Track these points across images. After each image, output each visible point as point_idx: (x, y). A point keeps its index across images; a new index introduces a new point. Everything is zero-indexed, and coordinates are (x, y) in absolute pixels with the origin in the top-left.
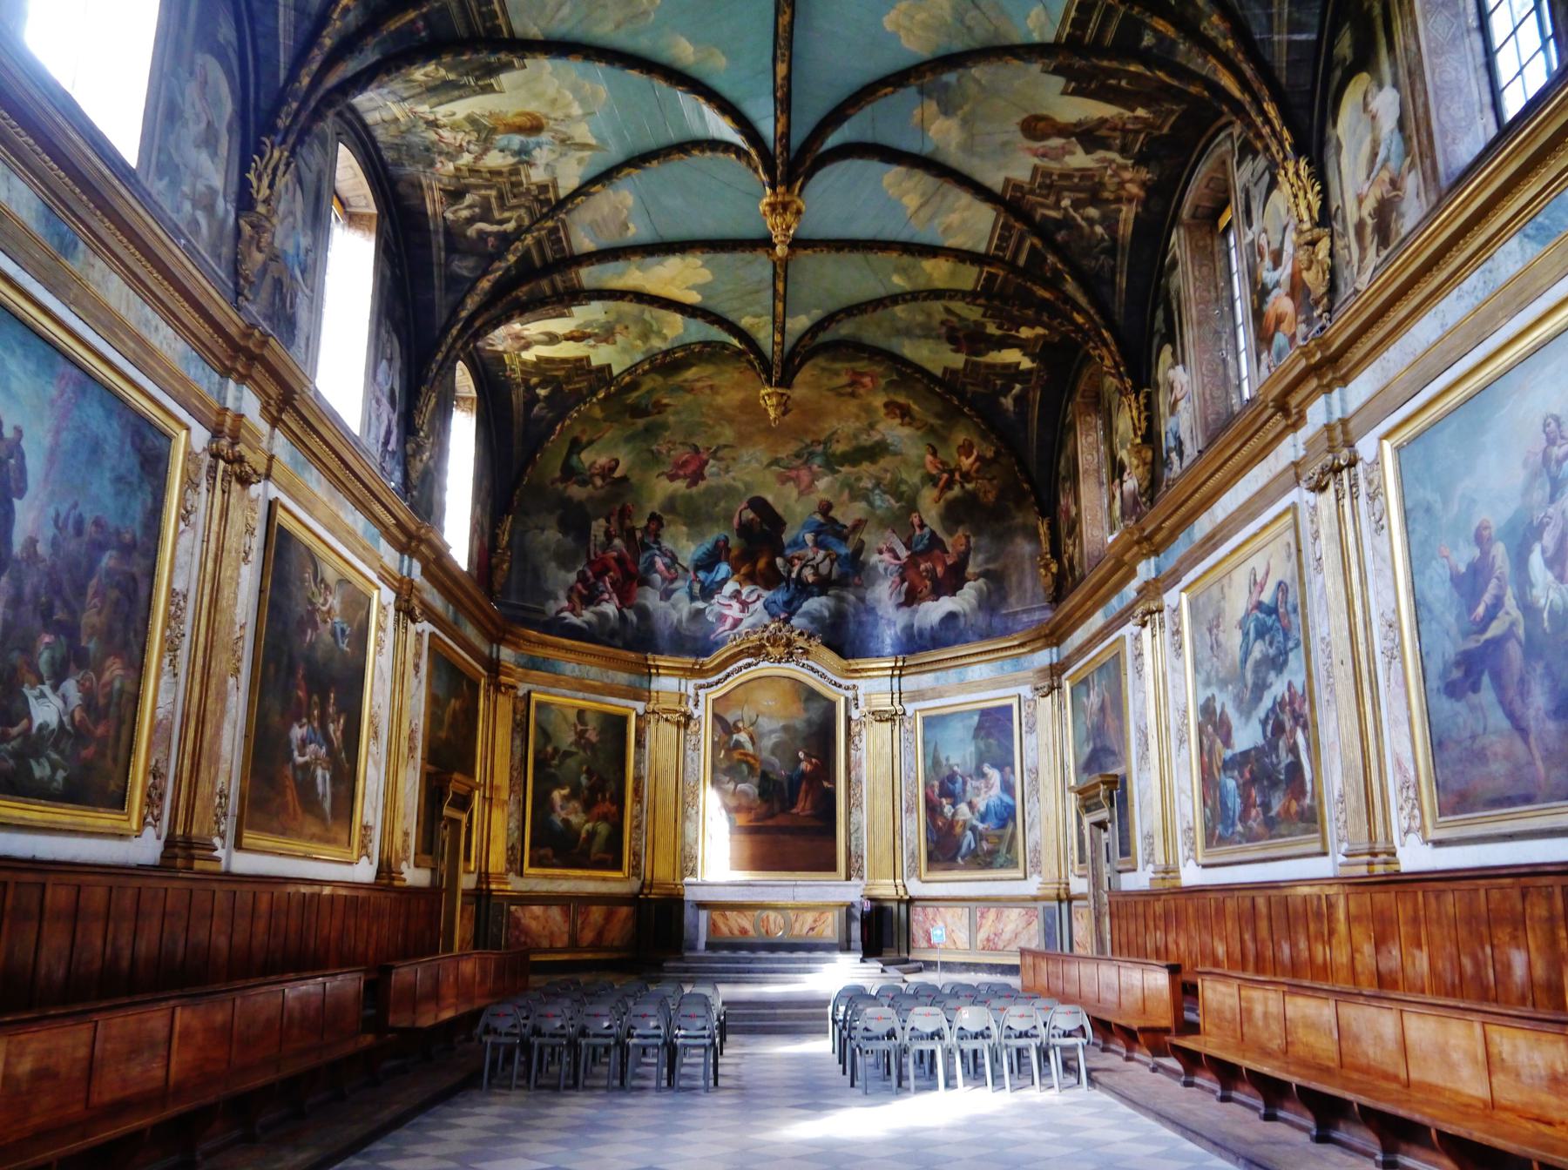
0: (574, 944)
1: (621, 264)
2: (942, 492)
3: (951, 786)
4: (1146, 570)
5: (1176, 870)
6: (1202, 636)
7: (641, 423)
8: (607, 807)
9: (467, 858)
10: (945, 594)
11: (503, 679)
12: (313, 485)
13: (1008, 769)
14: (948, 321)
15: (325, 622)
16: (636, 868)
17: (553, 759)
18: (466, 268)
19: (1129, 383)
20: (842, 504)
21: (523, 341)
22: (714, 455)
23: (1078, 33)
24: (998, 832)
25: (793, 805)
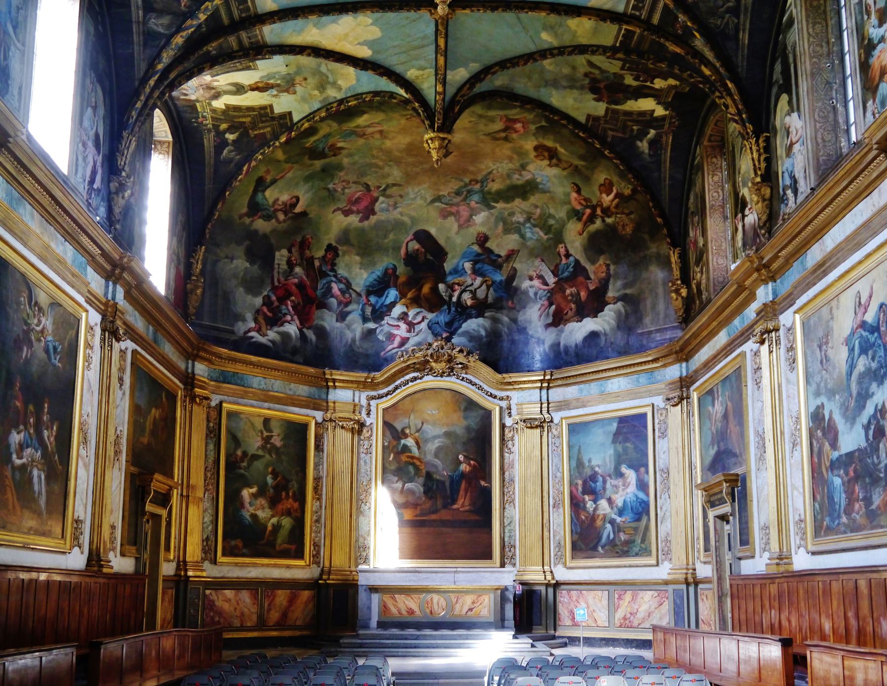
0: (261, 624)
1: (300, 22)
2: (586, 225)
3: (593, 485)
4: (764, 294)
5: (789, 557)
6: (813, 352)
7: (318, 164)
8: (290, 503)
9: (168, 549)
10: (588, 316)
11: (198, 391)
12: (27, 219)
13: (642, 470)
14: (590, 73)
15: (39, 340)
16: (316, 556)
17: (243, 461)
18: (162, 25)
19: (750, 128)
20: (497, 237)
21: (213, 91)
22: (384, 193)
24: (634, 525)
25: (454, 501)
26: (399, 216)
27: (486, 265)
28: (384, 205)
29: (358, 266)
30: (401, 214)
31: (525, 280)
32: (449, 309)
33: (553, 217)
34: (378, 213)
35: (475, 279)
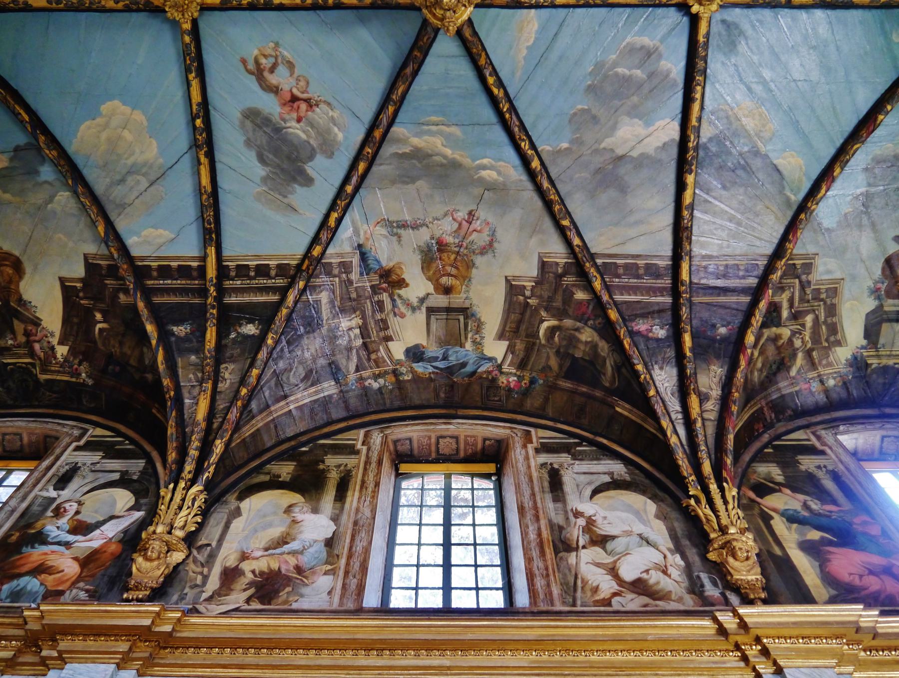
23: (155, 274)
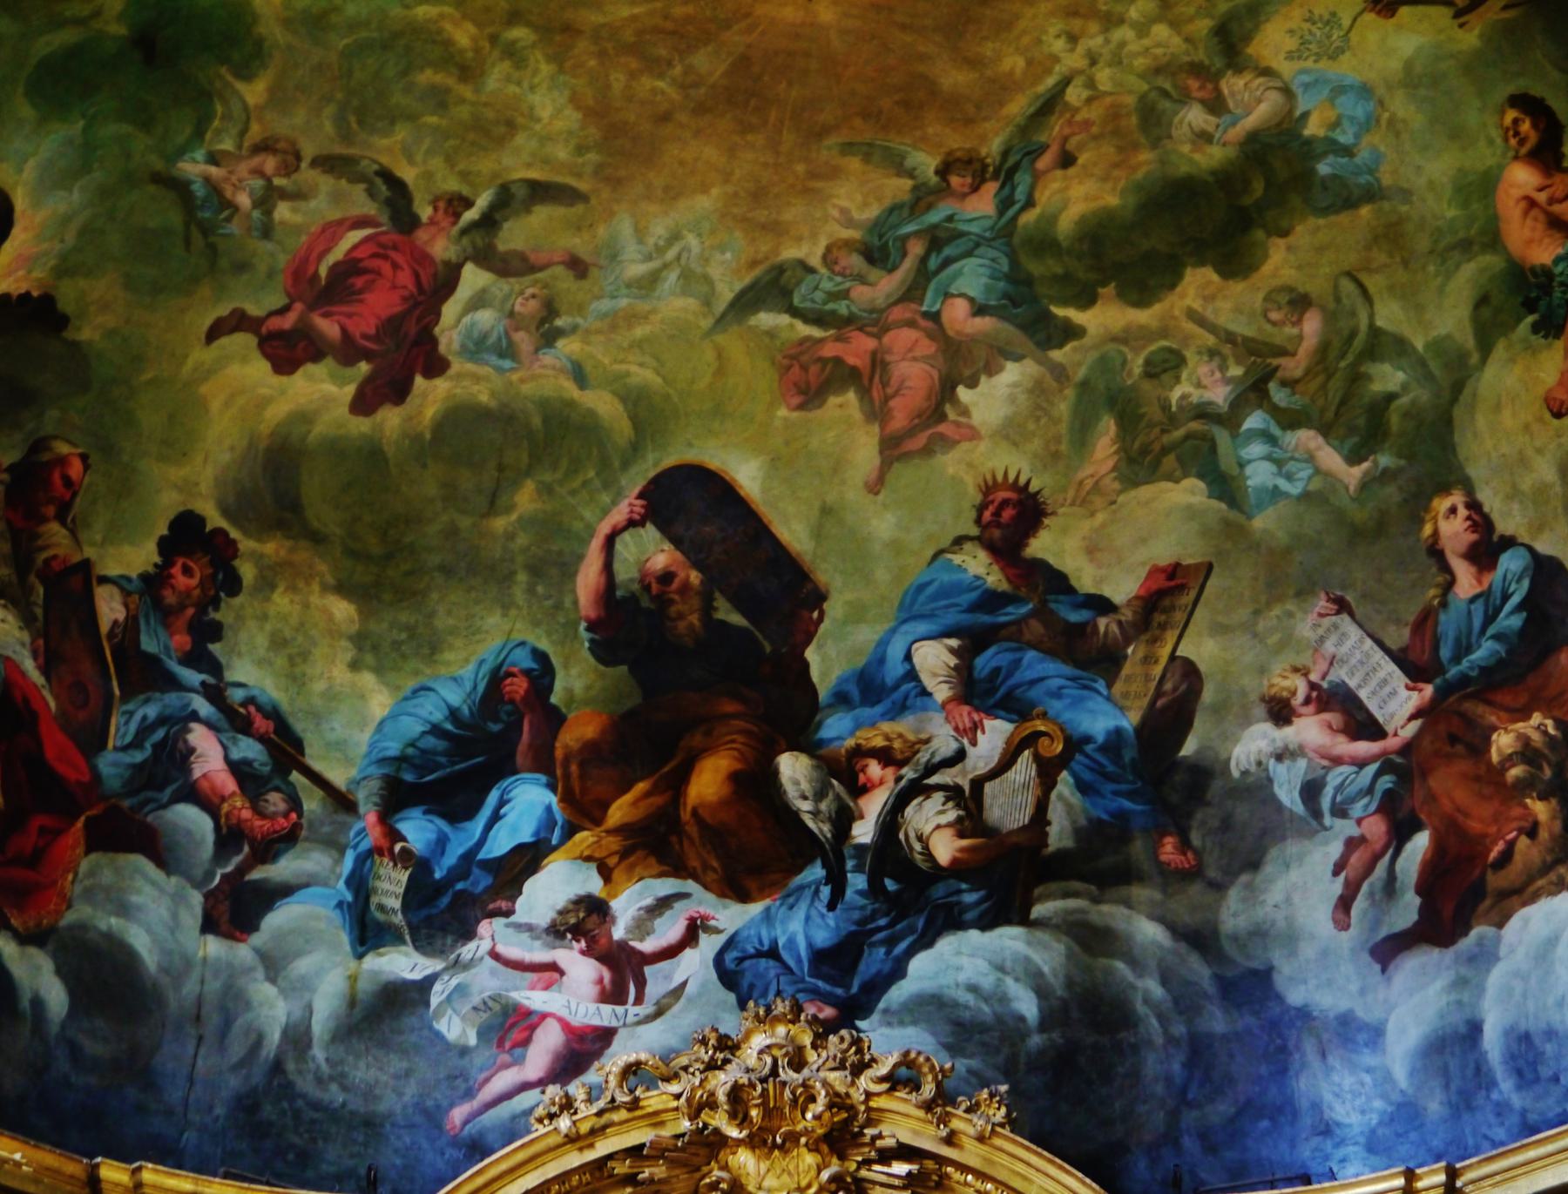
26: (570, 389)
27: (1031, 655)
28: (485, 318)
29: (346, 652)
30: (579, 375)
31: (1247, 721)
32: (837, 881)
33: (1400, 347)
34: (457, 365)
35: (972, 731)
